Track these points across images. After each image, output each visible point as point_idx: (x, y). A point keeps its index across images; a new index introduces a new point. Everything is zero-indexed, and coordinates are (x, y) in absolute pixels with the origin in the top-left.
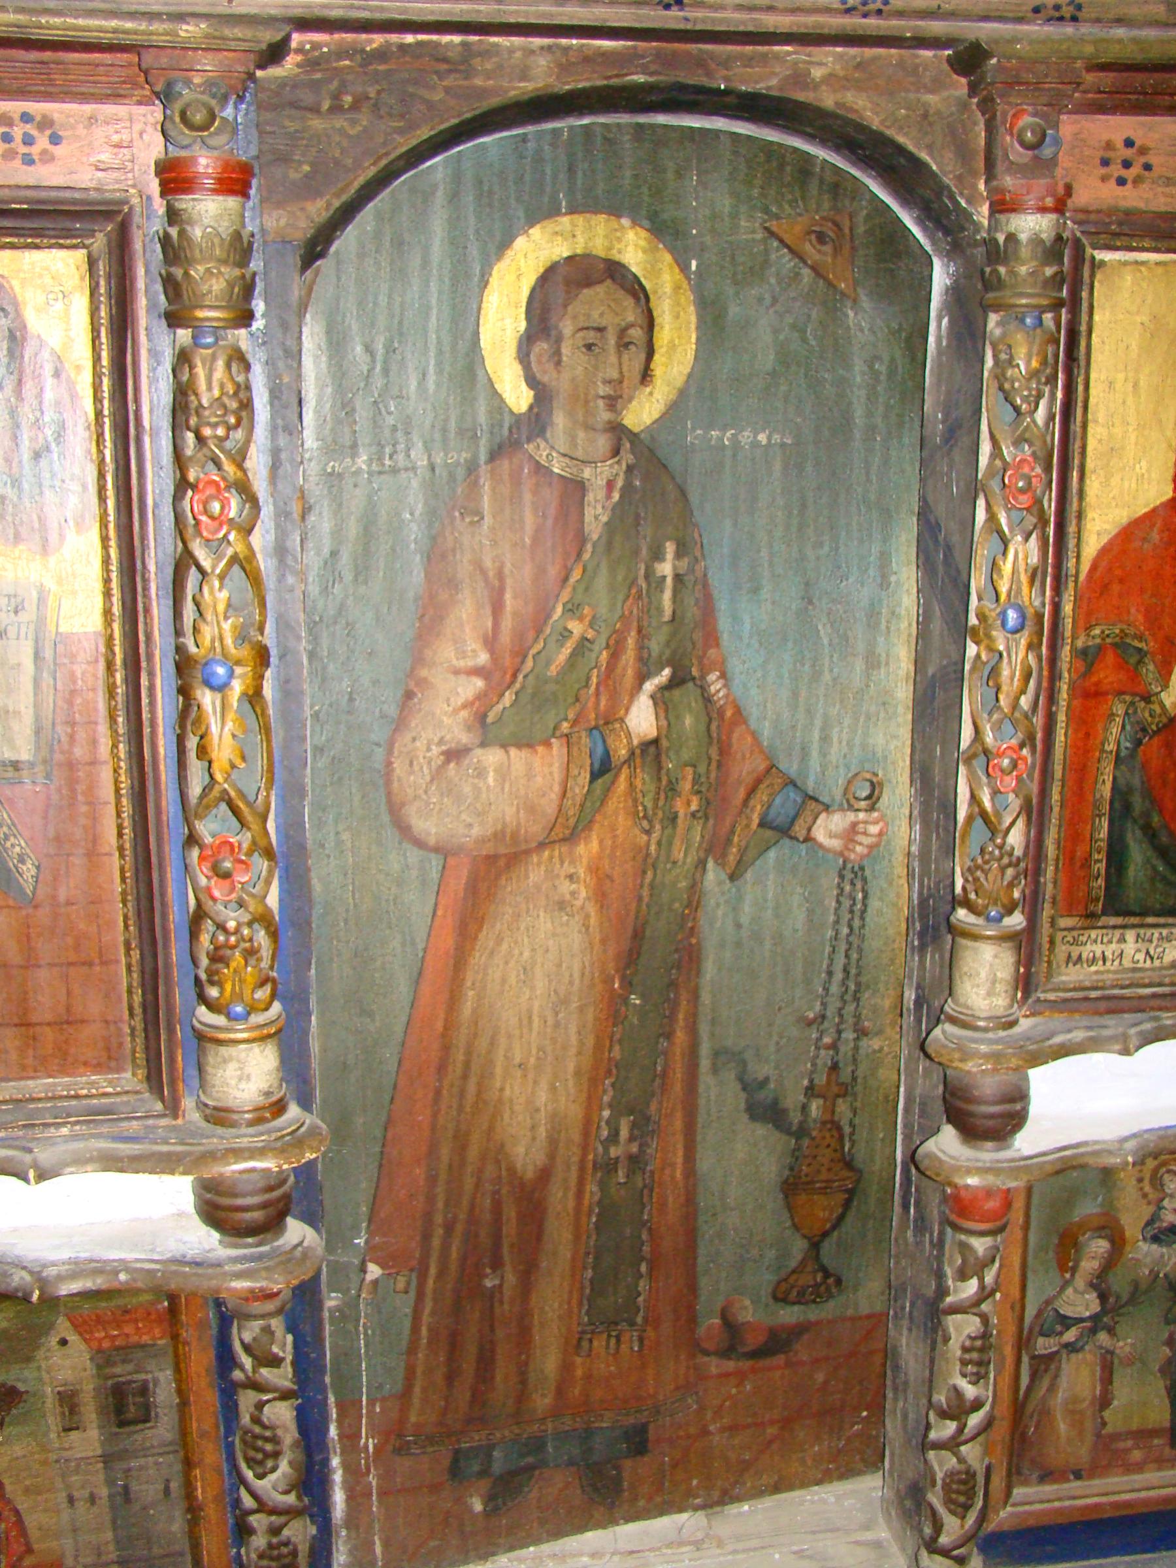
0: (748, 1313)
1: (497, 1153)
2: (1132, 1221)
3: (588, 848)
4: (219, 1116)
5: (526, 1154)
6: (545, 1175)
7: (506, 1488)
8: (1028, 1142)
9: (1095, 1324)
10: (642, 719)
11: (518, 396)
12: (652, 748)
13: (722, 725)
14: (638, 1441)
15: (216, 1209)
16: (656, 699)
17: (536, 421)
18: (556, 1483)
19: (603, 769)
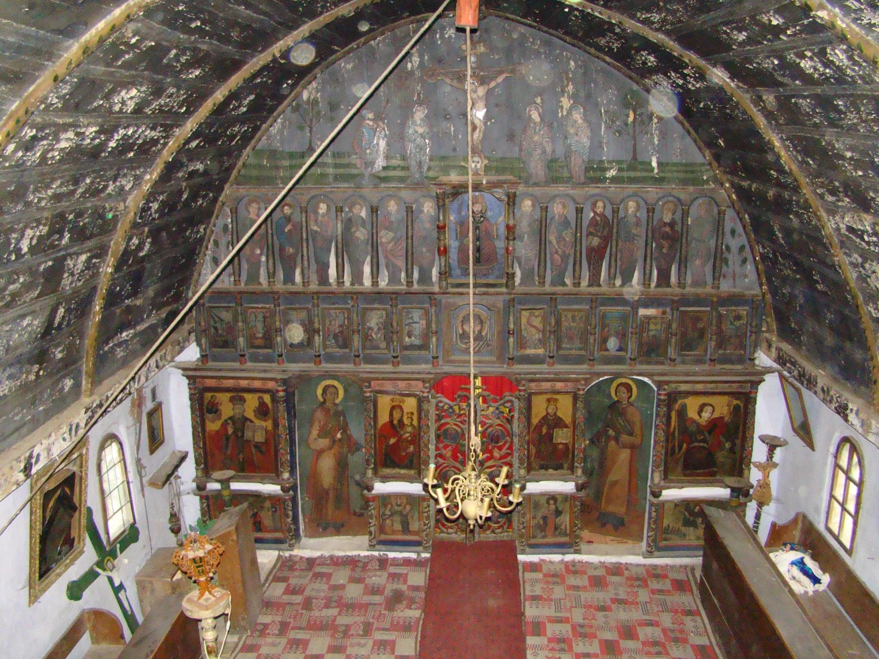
0: (357, 510)
1: (322, 485)
2: (394, 503)
3: (333, 451)
4: (283, 480)
5: (326, 486)
6: (329, 490)
7: (325, 529)
8: (373, 492)
9: (390, 516)
10: (339, 436)
11: (322, 400)
12: (340, 440)
13: (350, 437)
14: (343, 526)
15: (283, 489)
16: (341, 434)
17: (324, 402)
18: (331, 529)
19: (334, 441)
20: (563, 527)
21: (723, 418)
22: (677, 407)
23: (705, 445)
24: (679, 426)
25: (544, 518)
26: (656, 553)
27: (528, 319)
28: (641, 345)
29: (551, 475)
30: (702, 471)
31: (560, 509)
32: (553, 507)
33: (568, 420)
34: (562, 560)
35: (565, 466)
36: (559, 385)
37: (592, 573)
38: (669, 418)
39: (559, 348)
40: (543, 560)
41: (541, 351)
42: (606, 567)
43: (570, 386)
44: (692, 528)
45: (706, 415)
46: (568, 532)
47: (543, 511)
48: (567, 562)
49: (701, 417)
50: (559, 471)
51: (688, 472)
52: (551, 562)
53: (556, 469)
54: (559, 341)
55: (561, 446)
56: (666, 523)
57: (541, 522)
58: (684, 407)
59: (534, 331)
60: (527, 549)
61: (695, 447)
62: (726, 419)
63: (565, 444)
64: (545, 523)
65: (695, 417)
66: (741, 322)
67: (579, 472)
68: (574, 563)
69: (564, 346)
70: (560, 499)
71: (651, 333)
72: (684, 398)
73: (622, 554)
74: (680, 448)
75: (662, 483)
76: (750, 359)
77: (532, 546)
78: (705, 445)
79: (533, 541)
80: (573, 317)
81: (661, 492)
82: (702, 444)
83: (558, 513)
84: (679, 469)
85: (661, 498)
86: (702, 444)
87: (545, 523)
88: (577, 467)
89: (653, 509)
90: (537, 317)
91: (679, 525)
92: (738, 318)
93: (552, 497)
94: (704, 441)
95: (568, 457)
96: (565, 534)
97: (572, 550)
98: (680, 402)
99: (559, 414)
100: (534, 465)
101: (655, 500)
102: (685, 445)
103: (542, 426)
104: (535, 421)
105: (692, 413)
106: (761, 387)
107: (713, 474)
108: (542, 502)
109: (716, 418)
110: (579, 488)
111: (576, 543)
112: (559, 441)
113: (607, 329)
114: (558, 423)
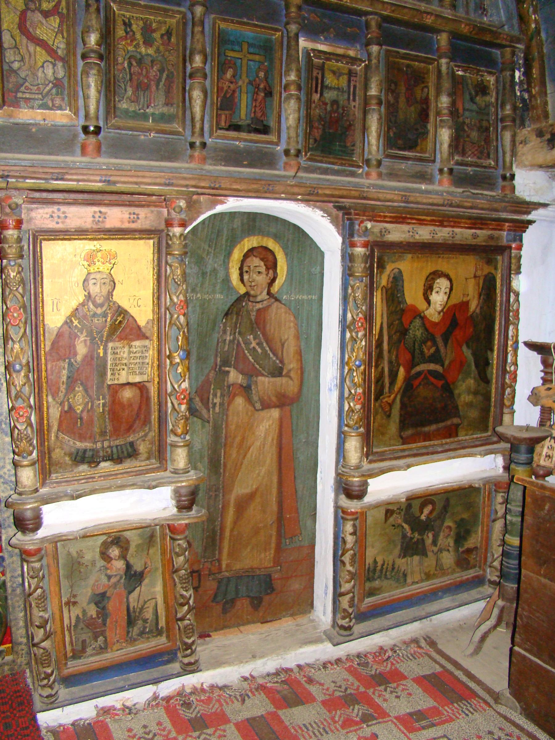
20: (149, 614)
21: (465, 305)
22: (384, 280)
23: (438, 368)
24: (390, 326)
25: (100, 599)
26: (358, 628)
27: (23, 16)
28: (309, 120)
29: (106, 477)
30: (434, 427)
31: (138, 566)
32: (120, 565)
33: (143, 313)
34: (155, 697)
35: (142, 448)
36: (116, 216)
37: (240, 712)
38: (371, 306)
39: (111, 109)
40: (106, 711)
41: (61, 117)
42: (262, 688)
43: (146, 217)
44: (416, 558)
45: (438, 298)
46: (162, 623)
47: (95, 580)
48: (168, 699)
49: (429, 302)
50: (128, 465)
51: (409, 432)
52: (128, 710)
53: (118, 460)
54: (109, 89)
55: (127, 394)
56: (370, 553)
57: (92, 611)
58: (397, 279)
59: (41, 55)
60: (63, 692)
61: (419, 374)
62: (473, 306)
63: (141, 387)
64: (103, 613)
65: (421, 305)
66: (487, 98)
67: (180, 458)
68: (183, 698)
69: (124, 105)
70: (134, 538)
71: (329, 95)
72: (400, 258)
73: (286, 648)
74: (393, 376)
75: (366, 466)
76: (504, 178)
77: (69, 681)
78: (438, 368)
79: (74, 666)
80: (147, 30)
81: (365, 485)
82: (432, 367)
83: (134, 578)
84: (393, 427)
85: (367, 499)
86: (432, 367)
87: (103, 613)
88: (174, 446)
89: (349, 527)
90: (46, 14)
91: (393, 557)
92: (483, 89)
93: (115, 539)
94: (436, 358)
95: (147, 421)
96: (159, 633)
97: (176, 667)
98: (389, 268)
99: (121, 298)
100: (57, 454)
101: (353, 506)
102: (402, 371)
103: (73, 337)
104: (54, 318)
105: (412, 295)
106: (528, 236)
107: (451, 432)
108: (88, 557)
109: (455, 305)
110: (187, 501)
111: (188, 646)
112: (123, 377)
113: (229, 74)
114: (122, 326)
